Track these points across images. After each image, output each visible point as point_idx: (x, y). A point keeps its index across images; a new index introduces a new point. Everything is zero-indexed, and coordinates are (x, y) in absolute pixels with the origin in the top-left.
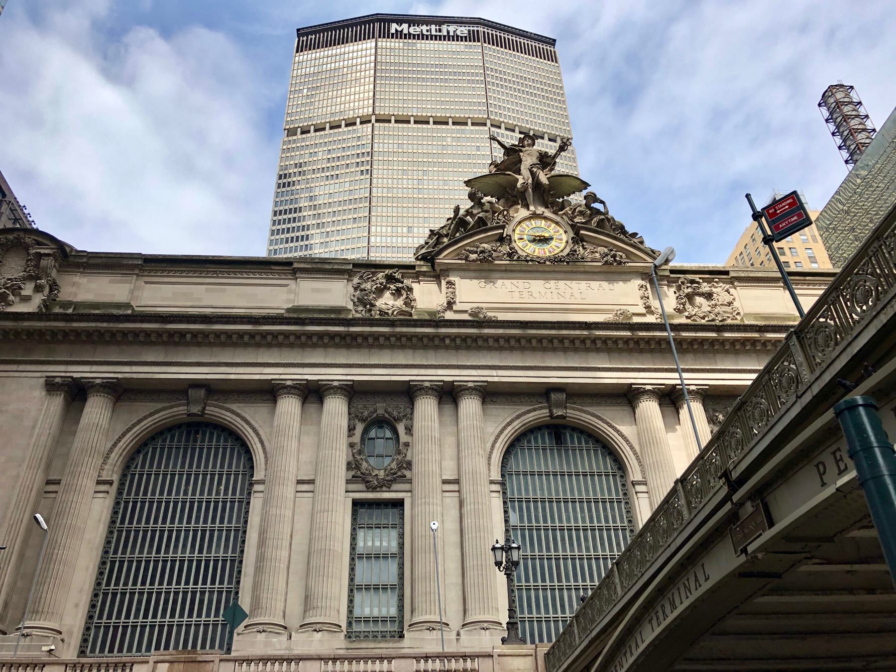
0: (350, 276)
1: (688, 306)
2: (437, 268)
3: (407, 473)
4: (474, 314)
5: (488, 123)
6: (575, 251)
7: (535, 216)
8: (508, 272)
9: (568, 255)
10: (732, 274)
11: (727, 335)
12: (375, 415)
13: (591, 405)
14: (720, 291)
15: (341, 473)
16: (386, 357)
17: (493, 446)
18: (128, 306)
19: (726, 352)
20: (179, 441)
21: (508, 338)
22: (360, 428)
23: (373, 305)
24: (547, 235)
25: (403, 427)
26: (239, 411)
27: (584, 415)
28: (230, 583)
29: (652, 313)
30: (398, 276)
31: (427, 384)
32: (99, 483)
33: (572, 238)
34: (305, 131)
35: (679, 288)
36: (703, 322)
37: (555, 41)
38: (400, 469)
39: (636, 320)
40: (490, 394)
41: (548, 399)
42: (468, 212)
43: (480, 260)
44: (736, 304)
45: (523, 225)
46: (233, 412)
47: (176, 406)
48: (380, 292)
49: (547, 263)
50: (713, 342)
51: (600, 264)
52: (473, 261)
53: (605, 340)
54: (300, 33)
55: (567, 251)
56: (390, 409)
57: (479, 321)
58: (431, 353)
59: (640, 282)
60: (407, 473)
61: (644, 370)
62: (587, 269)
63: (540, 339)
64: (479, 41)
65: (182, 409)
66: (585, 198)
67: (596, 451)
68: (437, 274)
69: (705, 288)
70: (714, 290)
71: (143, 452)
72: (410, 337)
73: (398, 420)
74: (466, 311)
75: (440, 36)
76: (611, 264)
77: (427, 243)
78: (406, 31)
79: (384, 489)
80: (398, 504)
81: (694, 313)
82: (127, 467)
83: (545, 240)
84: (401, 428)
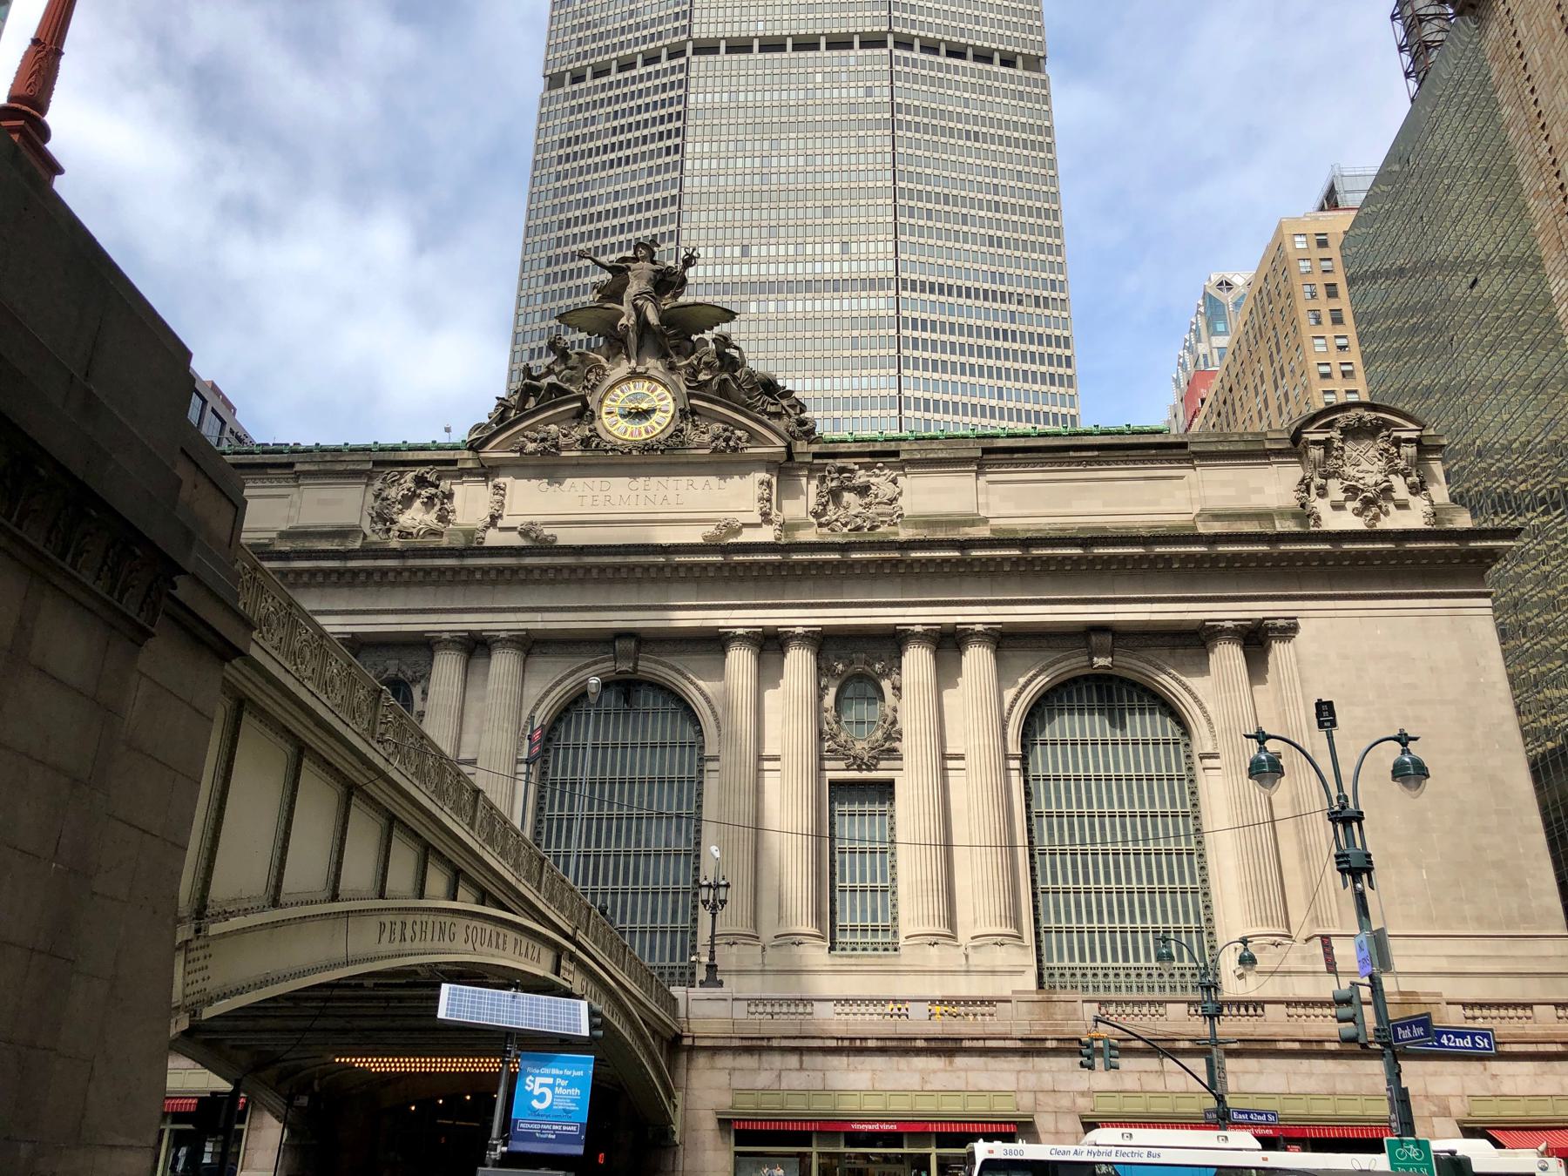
1: (831, 507)
4: (524, 533)
5: (890, 39)
6: (681, 431)
7: (634, 375)
8: (581, 468)
10: (903, 456)
11: (855, 556)
13: (671, 654)
14: (881, 482)
16: (398, 599)
21: (558, 569)
23: (393, 522)
24: (644, 406)
29: (770, 522)
30: (431, 478)
31: (446, 636)
34: (578, 78)
35: (823, 480)
44: (901, 501)
45: (618, 391)
48: (407, 501)
51: (707, 451)
52: (531, 453)
55: (670, 430)
56: (404, 668)
59: (764, 476)
63: (602, 569)
68: (487, 472)
69: (861, 477)
70: (873, 480)
72: (427, 571)
73: (415, 681)
74: (514, 529)
76: (723, 451)
83: (644, 414)
84: (417, 692)
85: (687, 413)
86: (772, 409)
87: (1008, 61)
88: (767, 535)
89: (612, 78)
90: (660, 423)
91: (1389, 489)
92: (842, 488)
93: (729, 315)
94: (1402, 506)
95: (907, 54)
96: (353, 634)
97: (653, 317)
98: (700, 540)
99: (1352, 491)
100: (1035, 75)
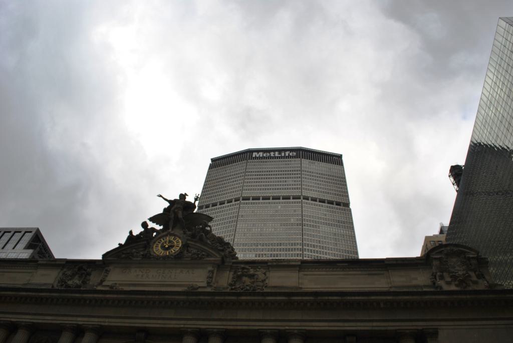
4: (111, 287)
5: (302, 197)
6: (182, 252)
9: (178, 254)
14: (260, 274)
23: (66, 283)
29: (211, 286)
35: (235, 272)
36: (242, 291)
37: (341, 155)
39: (200, 290)
51: (190, 259)
54: (213, 160)
55: (178, 252)
57: (112, 290)
61: (191, 320)
64: (299, 158)
70: (256, 273)
74: (108, 286)
75: (280, 157)
78: (261, 156)
81: (238, 286)
85: (185, 246)
86: (221, 248)
87: (338, 204)
89: (217, 207)
91: (469, 276)
92: (243, 275)
93: (211, 219)
94: (475, 283)
95: (306, 201)
96: (33, 322)
97: (180, 215)
99: (454, 278)
100: (346, 208)
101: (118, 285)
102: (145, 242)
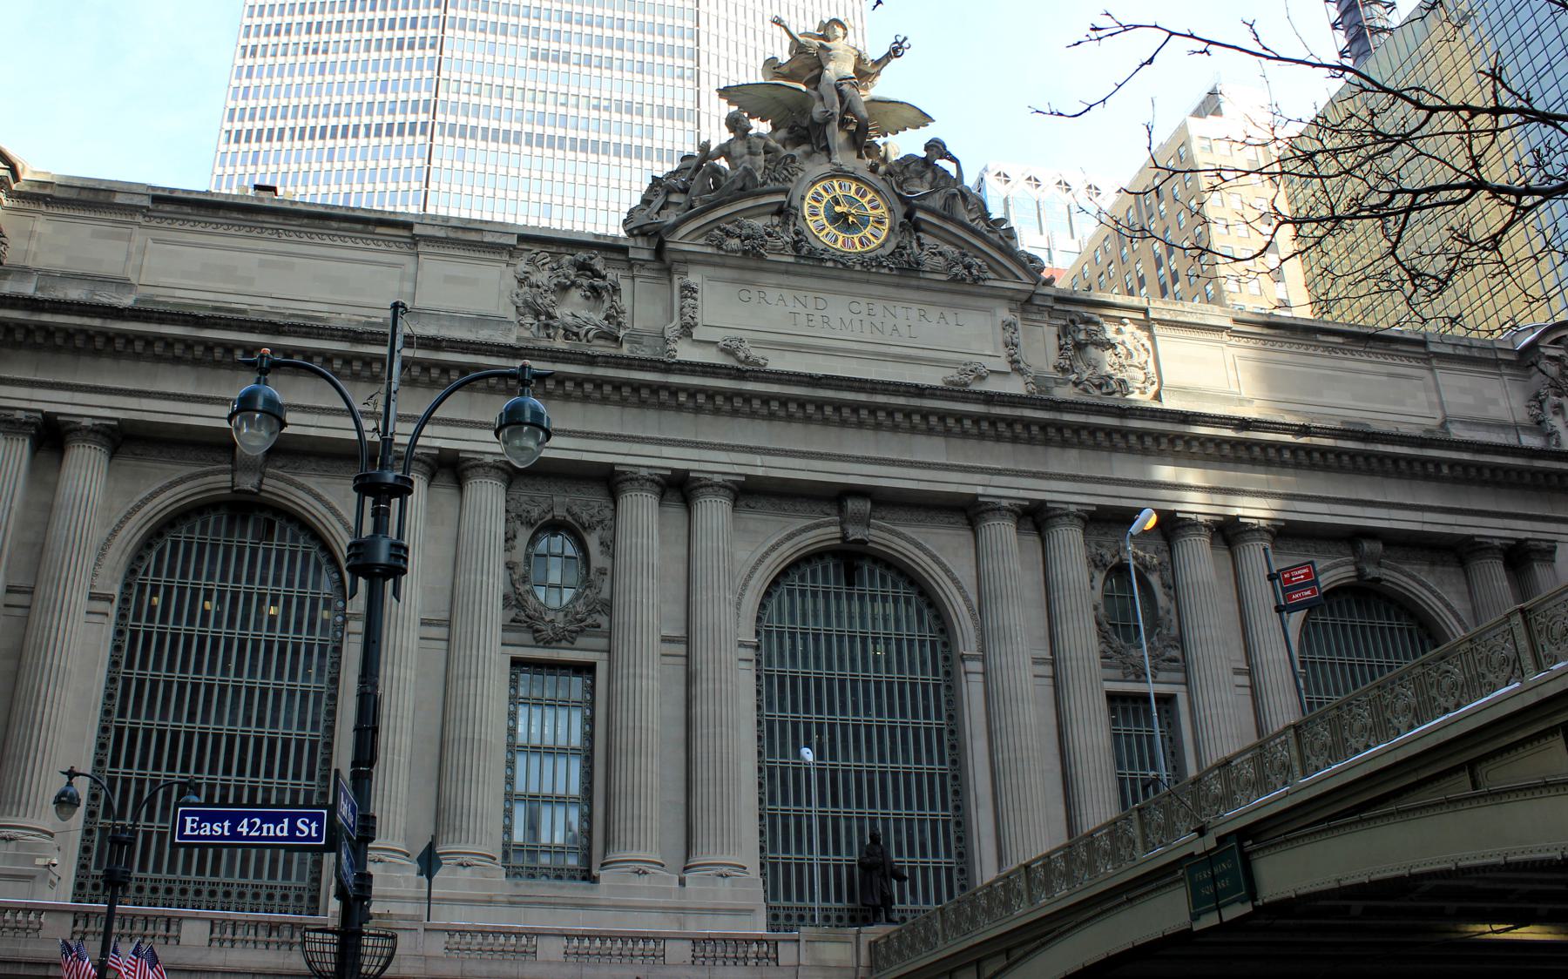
0: (511, 256)
2: (668, 257)
3: (603, 620)
4: (728, 351)
7: (840, 173)
12: (549, 517)
15: (495, 614)
17: (745, 585)
18: (124, 284)
19: (1130, 450)
20: (216, 532)
21: (784, 401)
22: (524, 535)
23: (550, 316)
25: (597, 542)
26: (320, 491)
27: (896, 539)
28: (310, 776)
30: (598, 265)
32: (93, 597)
33: (902, 224)
35: (1064, 332)
38: (590, 613)
39: (993, 386)
40: (748, 493)
41: (841, 510)
42: (724, 151)
43: (745, 252)
45: (819, 187)
46: (309, 491)
47: (213, 473)
48: (563, 289)
49: (858, 267)
50: (1109, 432)
51: (944, 277)
53: (943, 416)
55: (891, 247)
56: (576, 509)
58: (651, 416)
60: (603, 620)
61: (999, 472)
62: (923, 283)
63: (838, 406)
65: (224, 480)
66: (927, 147)
67: (908, 602)
71: (157, 548)
73: (590, 528)
77: (646, 201)
79: (564, 644)
80: (587, 669)
81: (1085, 376)
82: (132, 572)
88: (1015, 386)
90: (875, 237)
98: (939, 383)
101: (746, 345)
102: (781, 198)
